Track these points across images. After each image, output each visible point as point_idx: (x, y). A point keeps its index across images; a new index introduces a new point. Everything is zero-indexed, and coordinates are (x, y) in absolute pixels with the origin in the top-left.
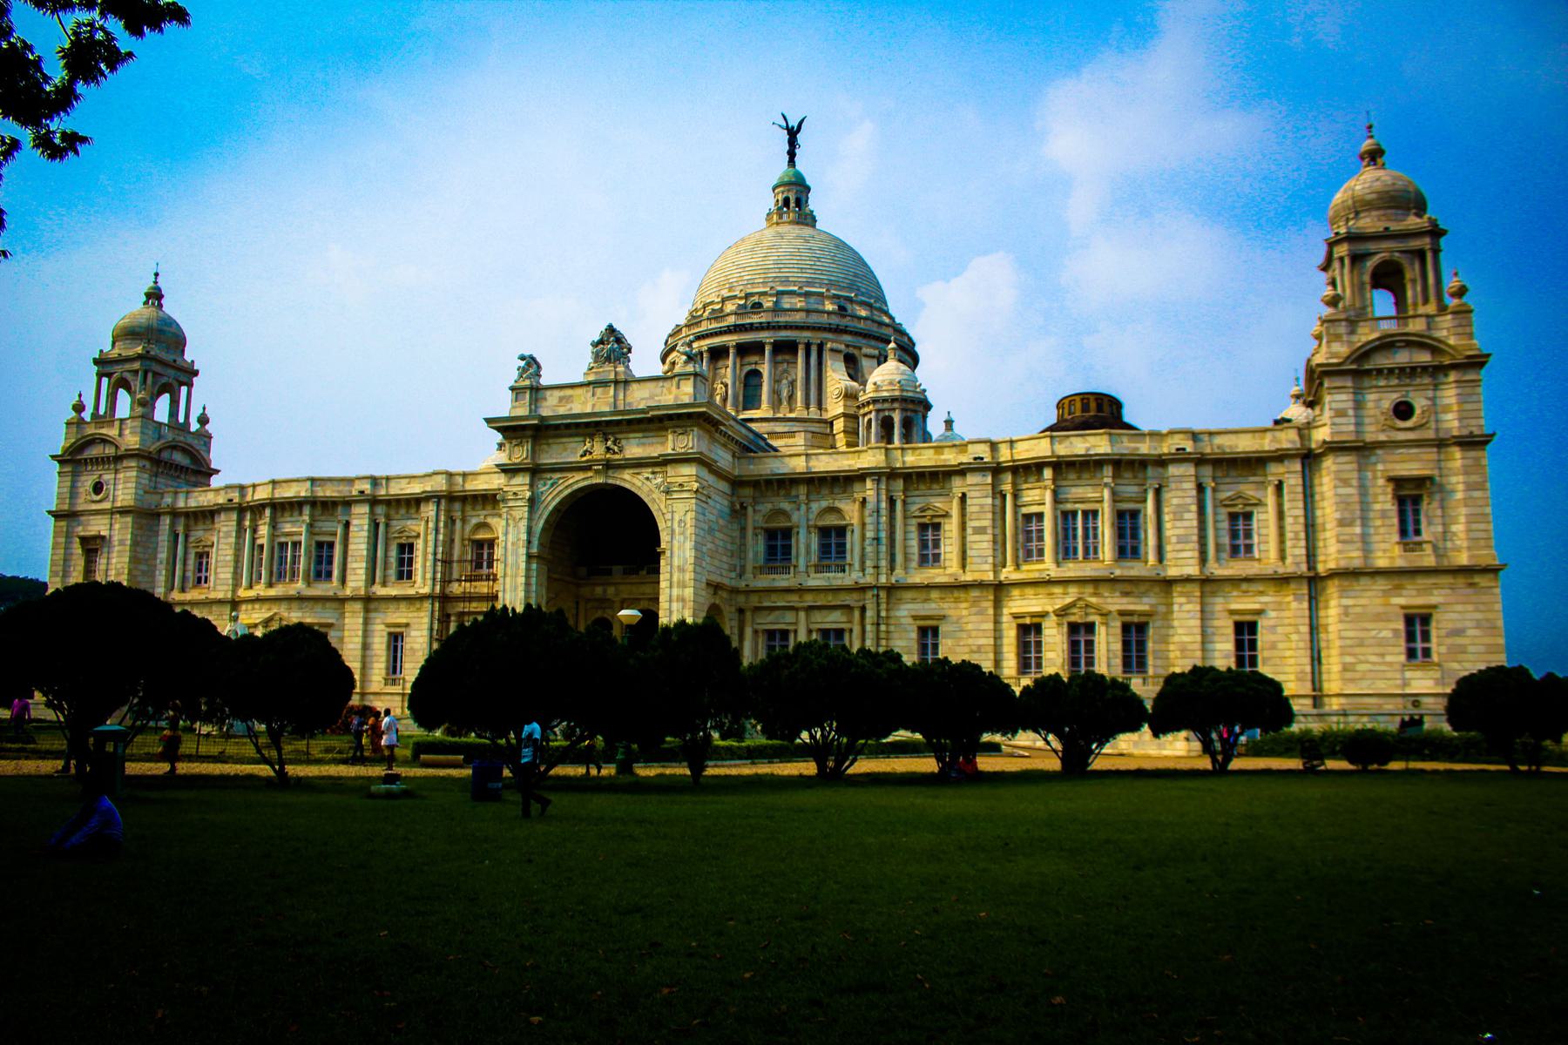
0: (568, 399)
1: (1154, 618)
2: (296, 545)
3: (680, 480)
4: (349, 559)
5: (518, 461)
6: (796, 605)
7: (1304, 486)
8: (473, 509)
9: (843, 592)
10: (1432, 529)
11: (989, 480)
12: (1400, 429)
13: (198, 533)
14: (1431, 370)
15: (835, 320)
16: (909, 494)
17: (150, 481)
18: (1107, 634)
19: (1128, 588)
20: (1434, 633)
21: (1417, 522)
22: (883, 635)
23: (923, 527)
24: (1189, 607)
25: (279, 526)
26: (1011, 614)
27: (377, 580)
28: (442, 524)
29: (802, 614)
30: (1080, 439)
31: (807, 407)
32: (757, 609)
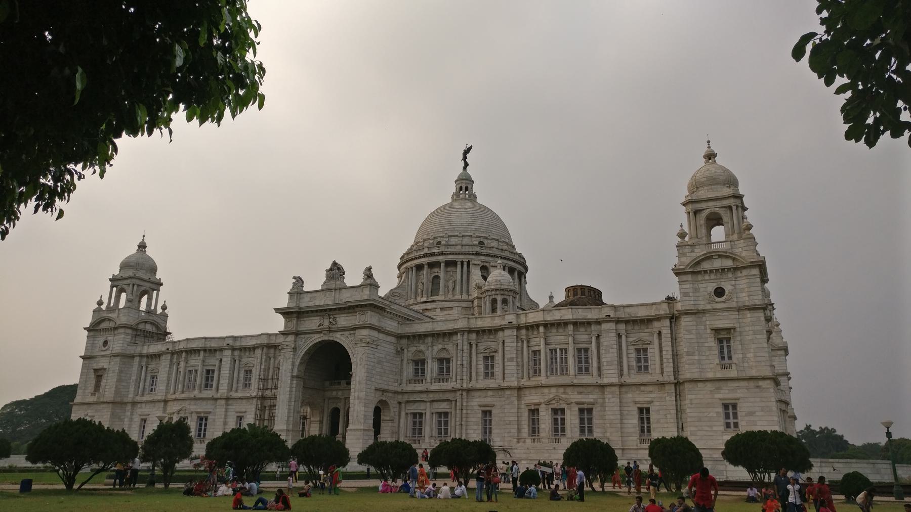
1: (596, 406)
2: (196, 371)
3: (361, 337)
4: (221, 379)
6: (425, 400)
7: (672, 334)
9: (447, 392)
10: (737, 356)
11: (515, 334)
12: (717, 302)
13: (152, 366)
14: (732, 270)
15: (477, 249)
16: (479, 341)
17: (132, 339)
18: (571, 415)
19: (581, 389)
20: (739, 414)
21: (729, 352)
22: (464, 415)
23: (486, 358)
24: (613, 400)
25: (189, 362)
26: (525, 404)
27: (233, 389)
28: (263, 360)
29: (428, 404)
30: (557, 311)
31: (462, 294)
32: (408, 402)
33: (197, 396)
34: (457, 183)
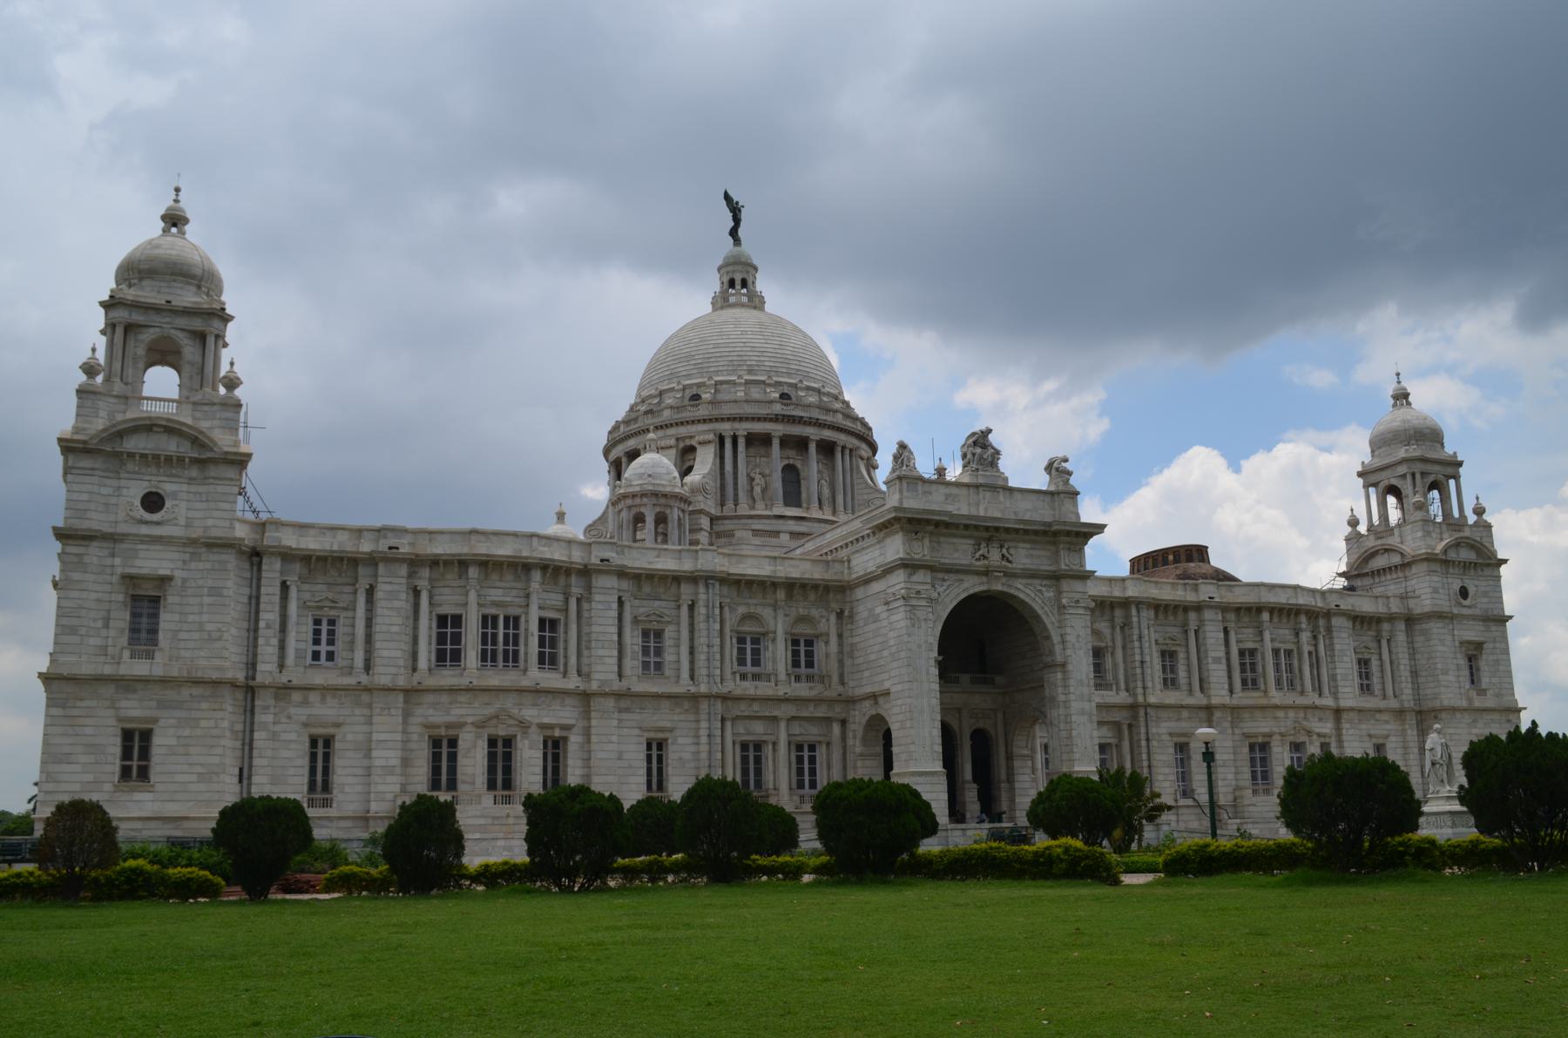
2: (513, 622)
3: (1077, 596)
11: (1220, 618)
24: (1351, 732)
26: (1244, 734)
28: (717, 611)
34: (722, 272)
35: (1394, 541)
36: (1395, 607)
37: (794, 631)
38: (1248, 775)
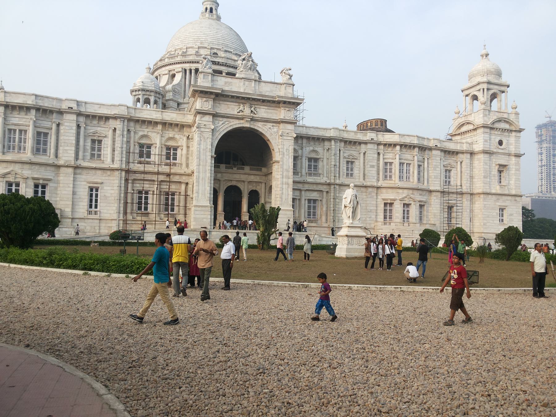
0: (230, 84)
3: (288, 131)
5: (206, 109)
6: (302, 189)
8: (141, 127)
9: (320, 185)
19: (420, 192)
22: (337, 203)
23: (348, 162)
25: (8, 119)
27: (81, 156)
28: (125, 133)
33: (32, 160)
35: (471, 119)
36: (465, 147)
37: (166, 144)
38: (382, 217)
